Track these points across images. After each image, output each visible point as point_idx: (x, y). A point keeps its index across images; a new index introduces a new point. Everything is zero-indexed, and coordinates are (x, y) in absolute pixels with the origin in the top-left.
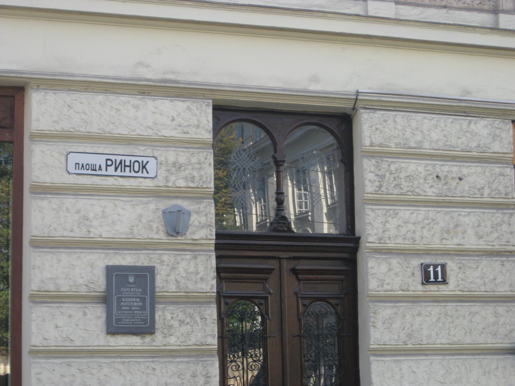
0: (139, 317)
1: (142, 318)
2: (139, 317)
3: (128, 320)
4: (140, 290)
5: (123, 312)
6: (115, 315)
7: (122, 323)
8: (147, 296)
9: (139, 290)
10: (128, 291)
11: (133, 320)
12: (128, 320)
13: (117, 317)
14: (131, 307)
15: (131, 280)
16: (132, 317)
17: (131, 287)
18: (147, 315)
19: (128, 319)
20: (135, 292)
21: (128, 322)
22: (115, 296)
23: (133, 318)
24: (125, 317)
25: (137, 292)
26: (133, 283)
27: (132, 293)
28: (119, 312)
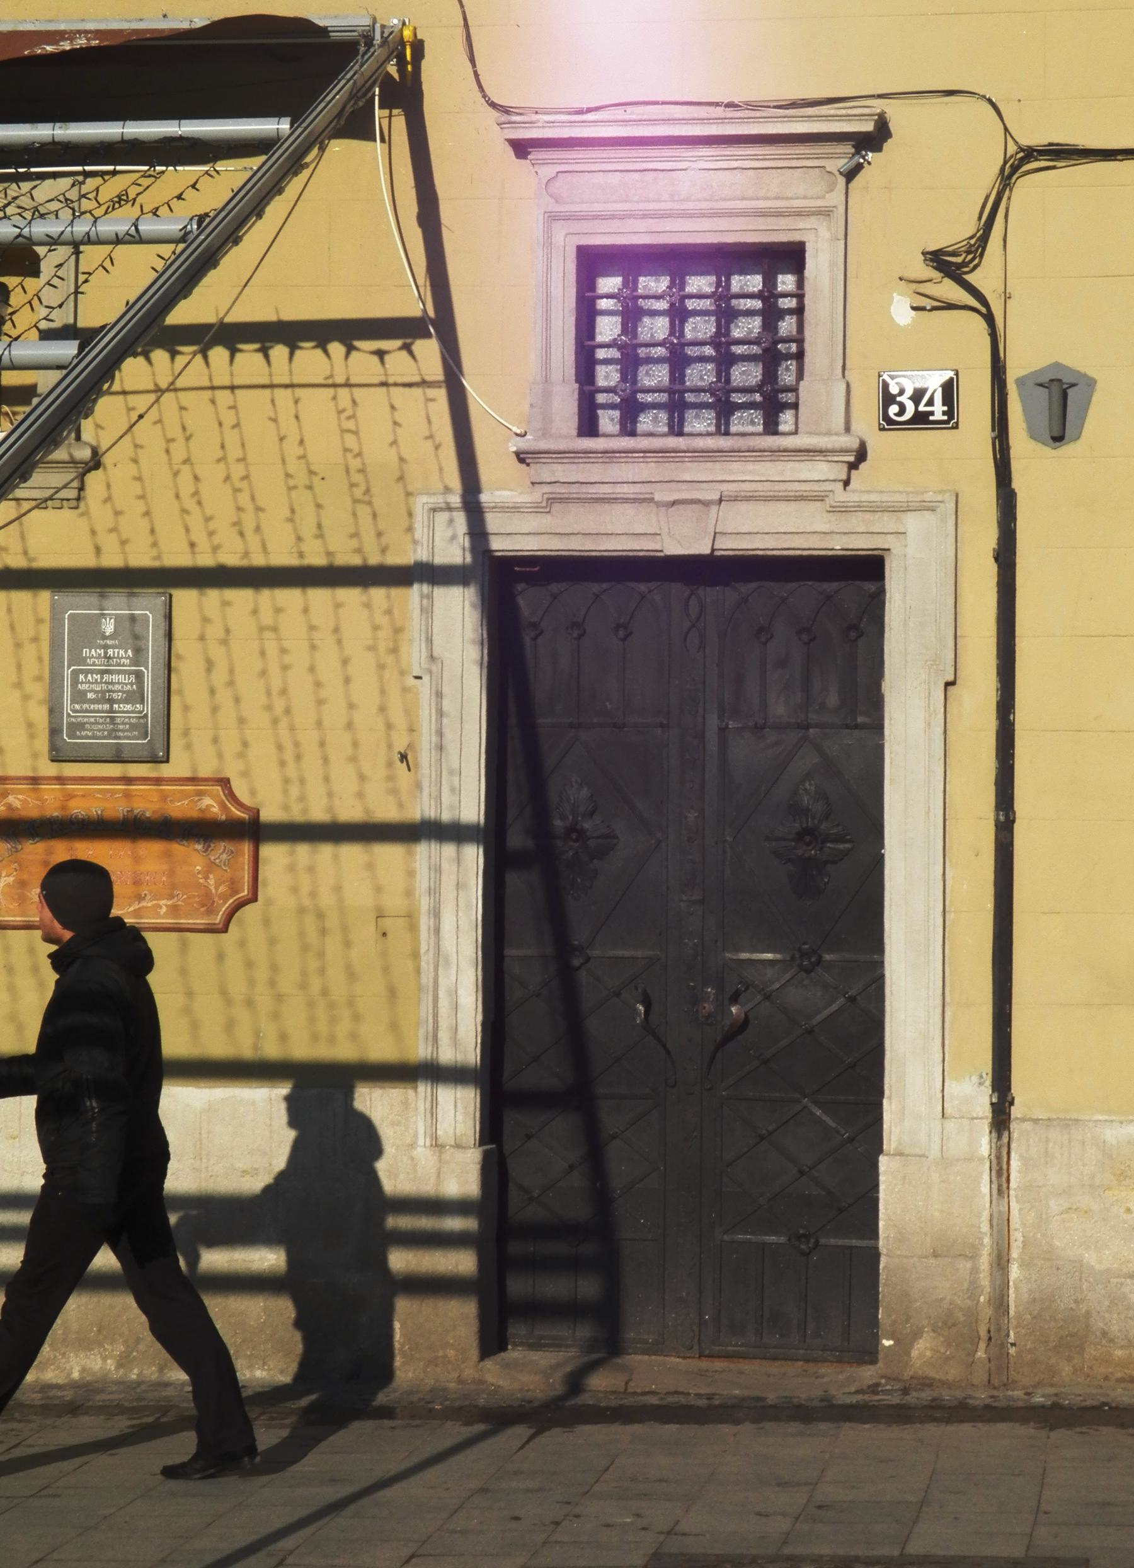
1: (133, 721)
3: (100, 727)
4: (130, 652)
5: (88, 706)
6: (69, 715)
7: (83, 733)
8: (147, 668)
9: (126, 652)
10: (100, 655)
12: (100, 727)
13: (73, 720)
15: (109, 627)
16: (108, 720)
19: (99, 724)
20: (118, 657)
21: (99, 731)
22: (69, 668)
25: (122, 658)
26: (111, 637)
28: (77, 707)
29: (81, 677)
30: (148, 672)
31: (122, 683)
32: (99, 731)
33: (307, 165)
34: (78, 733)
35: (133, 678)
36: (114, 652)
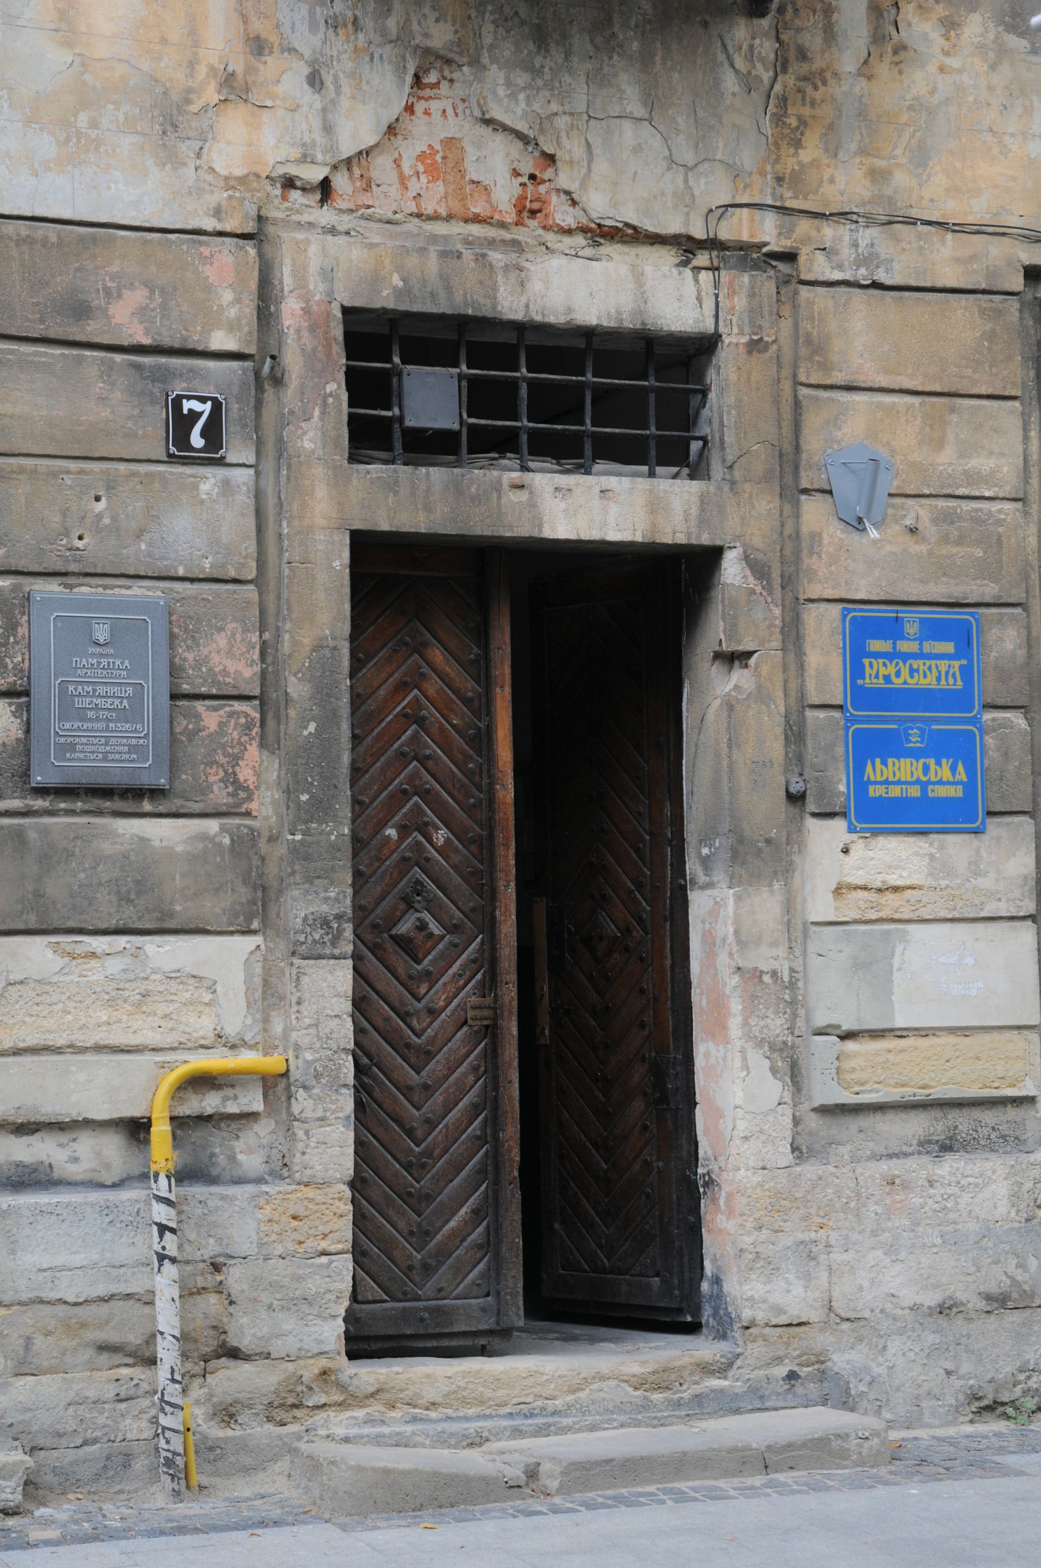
1: (134, 741)
2: (125, 741)
3: (94, 748)
12: (94, 748)
13: (62, 740)
17: (102, 655)
18: (146, 736)
21: (93, 752)
23: (106, 744)
24: (84, 740)
27: (105, 672)
29: (71, 688)
30: (148, 684)
32: (93, 752)
33: (561, 465)
34: (68, 755)
35: (130, 690)
36: (109, 663)
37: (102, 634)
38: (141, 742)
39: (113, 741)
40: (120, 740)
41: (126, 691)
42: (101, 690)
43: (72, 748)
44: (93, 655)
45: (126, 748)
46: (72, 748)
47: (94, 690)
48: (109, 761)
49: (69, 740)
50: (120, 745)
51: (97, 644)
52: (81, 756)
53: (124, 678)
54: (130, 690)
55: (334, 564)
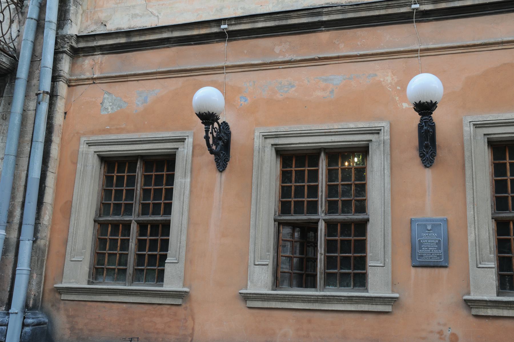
0: (436, 254)
1: (438, 254)
2: (436, 254)
3: (428, 256)
4: (436, 235)
6: (418, 253)
9: (435, 235)
10: (427, 235)
11: (431, 256)
12: (428, 256)
13: (419, 254)
14: (428, 248)
16: (430, 254)
17: (429, 233)
21: (428, 257)
23: (431, 255)
24: (425, 254)
27: (430, 237)
28: (421, 251)
29: (421, 241)
30: (442, 239)
31: (434, 243)
32: (428, 257)
35: (437, 241)
37: (429, 228)
38: (440, 254)
39: (433, 254)
40: (434, 254)
41: (436, 241)
42: (429, 241)
43: (422, 256)
44: (427, 233)
45: (436, 256)
46: (422, 256)
47: (428, 241)
48: (431, 259)
49: (421, 254)
50: (435, 255)
51: (429, 230)
52: (425, 258)
53: (435, 238)
54: (437, 241)
55: (398, 98)
